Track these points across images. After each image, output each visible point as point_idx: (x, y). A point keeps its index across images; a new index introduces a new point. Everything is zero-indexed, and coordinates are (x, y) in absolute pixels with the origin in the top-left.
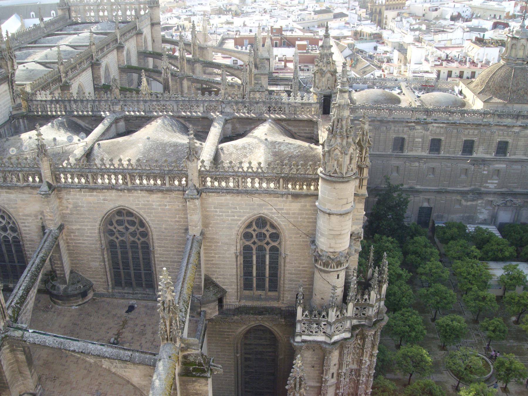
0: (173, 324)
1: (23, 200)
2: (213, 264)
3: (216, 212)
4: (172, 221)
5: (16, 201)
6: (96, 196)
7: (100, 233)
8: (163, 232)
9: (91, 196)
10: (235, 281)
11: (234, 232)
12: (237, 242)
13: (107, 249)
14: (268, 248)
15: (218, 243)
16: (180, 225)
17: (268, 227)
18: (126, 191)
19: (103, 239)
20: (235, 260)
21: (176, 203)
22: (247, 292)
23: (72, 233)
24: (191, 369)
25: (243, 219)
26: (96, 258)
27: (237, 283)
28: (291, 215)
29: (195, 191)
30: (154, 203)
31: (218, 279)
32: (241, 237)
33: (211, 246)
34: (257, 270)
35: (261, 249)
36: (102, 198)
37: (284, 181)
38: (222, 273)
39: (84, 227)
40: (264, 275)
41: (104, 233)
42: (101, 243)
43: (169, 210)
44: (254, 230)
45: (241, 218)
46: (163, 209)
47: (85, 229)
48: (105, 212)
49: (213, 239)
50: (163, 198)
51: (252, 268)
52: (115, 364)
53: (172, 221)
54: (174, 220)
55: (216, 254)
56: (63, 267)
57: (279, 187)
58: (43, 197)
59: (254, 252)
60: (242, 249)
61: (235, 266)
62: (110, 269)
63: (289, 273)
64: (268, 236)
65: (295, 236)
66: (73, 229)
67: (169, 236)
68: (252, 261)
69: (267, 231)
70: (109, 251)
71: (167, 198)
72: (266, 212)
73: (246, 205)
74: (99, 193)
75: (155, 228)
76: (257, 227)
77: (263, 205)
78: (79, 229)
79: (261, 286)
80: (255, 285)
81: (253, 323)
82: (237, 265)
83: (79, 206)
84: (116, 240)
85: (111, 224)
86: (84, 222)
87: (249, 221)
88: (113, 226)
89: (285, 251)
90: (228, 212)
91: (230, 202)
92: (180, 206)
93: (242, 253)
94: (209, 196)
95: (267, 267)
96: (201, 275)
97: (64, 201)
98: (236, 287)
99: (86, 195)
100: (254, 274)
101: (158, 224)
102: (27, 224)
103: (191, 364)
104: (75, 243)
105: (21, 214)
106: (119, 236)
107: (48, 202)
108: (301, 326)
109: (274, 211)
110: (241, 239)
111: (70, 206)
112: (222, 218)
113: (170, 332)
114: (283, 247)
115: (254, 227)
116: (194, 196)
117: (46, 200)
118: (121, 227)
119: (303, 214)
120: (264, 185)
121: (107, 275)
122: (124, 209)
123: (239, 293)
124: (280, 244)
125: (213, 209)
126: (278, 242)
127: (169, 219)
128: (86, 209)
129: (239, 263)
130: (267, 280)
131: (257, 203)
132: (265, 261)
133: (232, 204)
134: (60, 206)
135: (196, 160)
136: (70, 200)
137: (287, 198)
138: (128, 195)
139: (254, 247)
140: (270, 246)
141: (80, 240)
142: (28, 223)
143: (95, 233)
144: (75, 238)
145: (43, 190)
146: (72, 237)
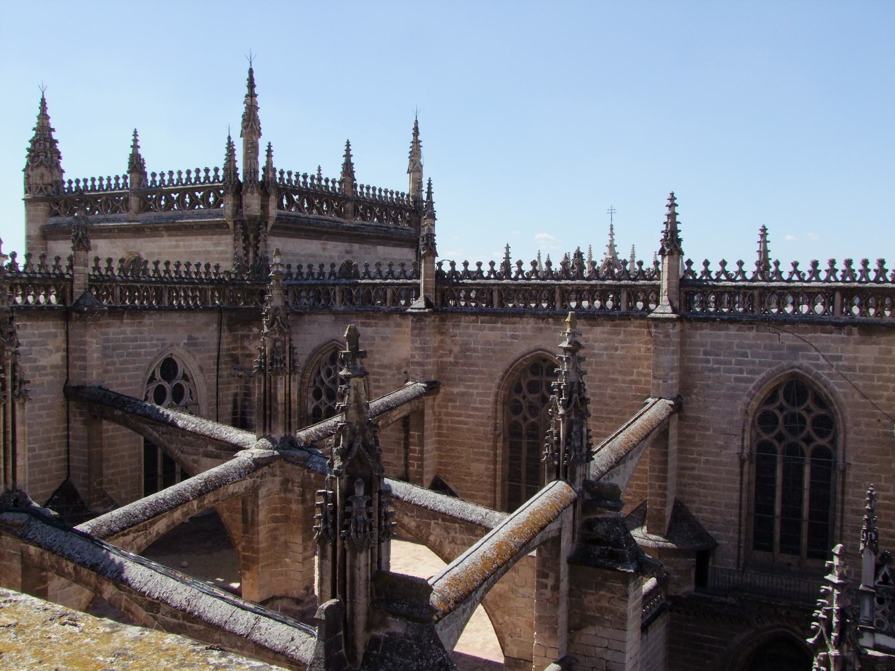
0: (572, 434)
1: (383, 339)
2: (693, 477)
3: (708, 361)
4: (624, 382)
5: (374, 339)
6: (501, 329)
7: (496, 402)
8: (606, 405)
9: (492, 329)
10: (735, 519)
11: (740, 407)
12: (744, 430)
13: (504, 439)
14: (808, 450)
15: (707, 429)
16: (638, 390)
17: (809, 402)
18: (550, 320)
19: (500, 415)
20: (738, 470)
21: (636, 345)
22: (760, 555)
23: (451, 401)
24: (597, 553)
25: (758, 378)
26: (483, 454)
27: (740, 526)
28: (858, 373)
29: (669, 309)
30: (596, 344)
31: (701, 512)
32: (753, 421)
33: (693, 436)
34: (783, 501)
35: (793, 450)
36: (509, 333)
37: (843, 297)
38: (710, 499)
39: (471, 390)
40: (798, 514)
41: (504, 404)
42: (496, 424)
43: (623, 358)
44: (781, 409)
45: (756, 376)
46: (611, 357)
47: (472, 395)
48: (511, 360)
49: (698, 419)
50: (614, 334)
51: (774, 496)
52: (452, 534)
53: (624, 382)
54: (628, 378)
55: (700, 455)
56: (421, 459)
57: (833, 313)
58: (415, 320)
59: (779, 457)
60: (755, 448)
61: (738, 486)
62: (503, 481)
63: (853, 511)
64: (809, 421)
65: (866, 419)
66: (453, 394)
67: (615, 413)
68: (774, 480)
69: (809, 411)
70: (507, 444)
71: (619, 334)
72: (805, 363)
73: (765, 348)
74: (506, 323)
75: (593, 394)
76: (787, 401)
77: (801, 348)
78: (463, 395)
79: (790, 544)
80: (777, 538)
81: (768, 624)
82: (741, 484)
83: (469, 350)
84: (522, 422)
85: (519, 389)
86: (473, 380)
87: (770, 385)
88: (522, 395)
89: (844, 457)
90: (731, 363)
91: (736, 341)
92: (642, 350)
93: (754, 457)
94: (696, 329)
95: (806, 495)
96: (665, 488)
97: (448, 340)
98: (737, 536)
99: (484, 329)
100: (778, 510)
101: (599, 387)
102: (382, 384)
103: (598, 542)
104: (453, 422)
105: (376, 363)
106: (528, 416)
107: (421, 329)
108: (872, 604)
109: (822, 361)
110: (753, 426)
111: (456, 349)
112: (717, 374)
113: (566, 451)
114: (840, 446)
115: (781, 399)
116: (667, 316)
117: (418, 325)
118: (533, 396)
119: (884, 370)
120: (804, 309)
121: (495, 492)
122: (545, 360)
123: (742, 552)
124: (833, 442)
125: (702, 356)
126: (830, 438)
127: (620, 378)
128: (480, 355)
129: (746, 478)
130: (805, 526)
131: (787, 343)
132: (801, 483)
133: (738, 346)
134: (440, 347)
135: (676, 256)
136: (457, 338)
137: (850, 333)
138: (553, 327)
139: (779, 447)
140: (812, 446)
141: (460, 415)
142: (384, 381)
143: (488, 403)
144: (454, 411)
145: (416, 306)
146: (450, 410)
